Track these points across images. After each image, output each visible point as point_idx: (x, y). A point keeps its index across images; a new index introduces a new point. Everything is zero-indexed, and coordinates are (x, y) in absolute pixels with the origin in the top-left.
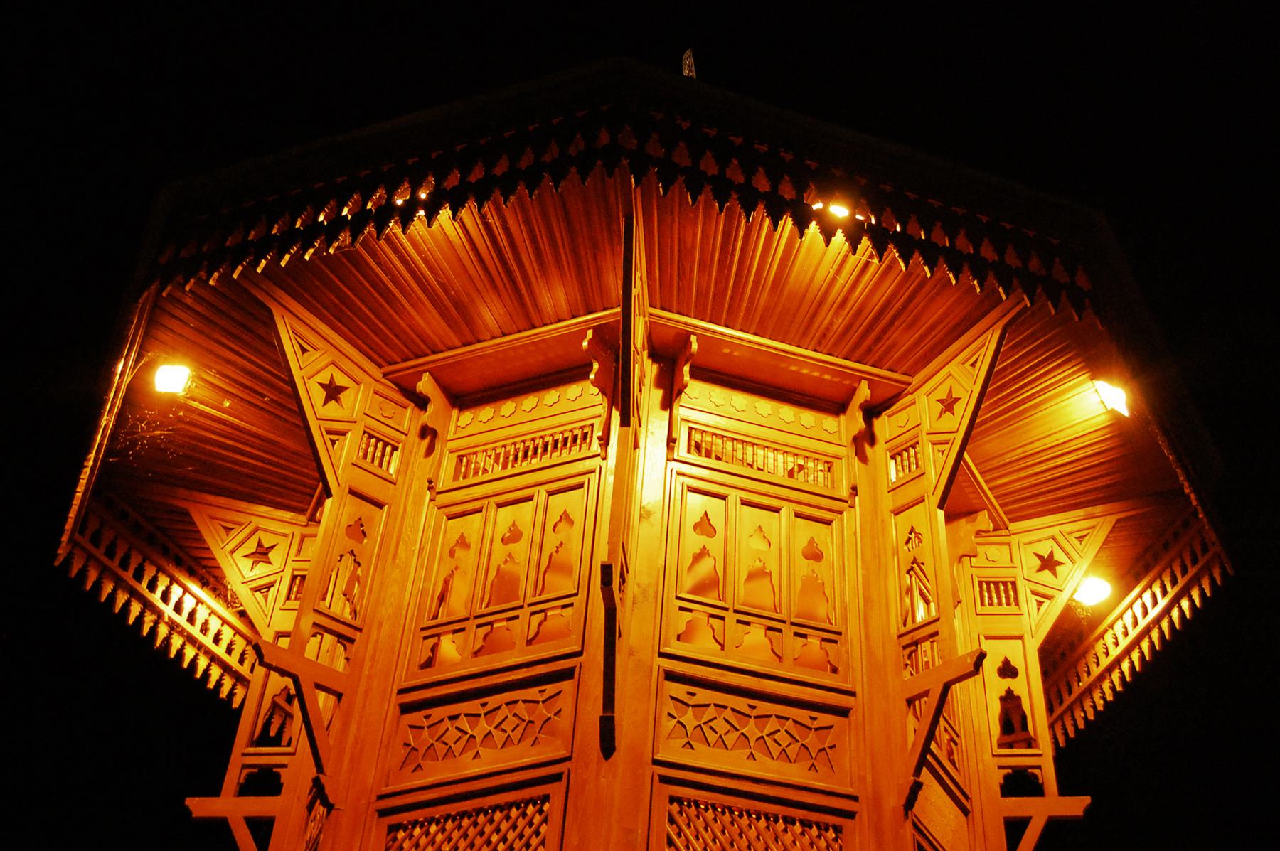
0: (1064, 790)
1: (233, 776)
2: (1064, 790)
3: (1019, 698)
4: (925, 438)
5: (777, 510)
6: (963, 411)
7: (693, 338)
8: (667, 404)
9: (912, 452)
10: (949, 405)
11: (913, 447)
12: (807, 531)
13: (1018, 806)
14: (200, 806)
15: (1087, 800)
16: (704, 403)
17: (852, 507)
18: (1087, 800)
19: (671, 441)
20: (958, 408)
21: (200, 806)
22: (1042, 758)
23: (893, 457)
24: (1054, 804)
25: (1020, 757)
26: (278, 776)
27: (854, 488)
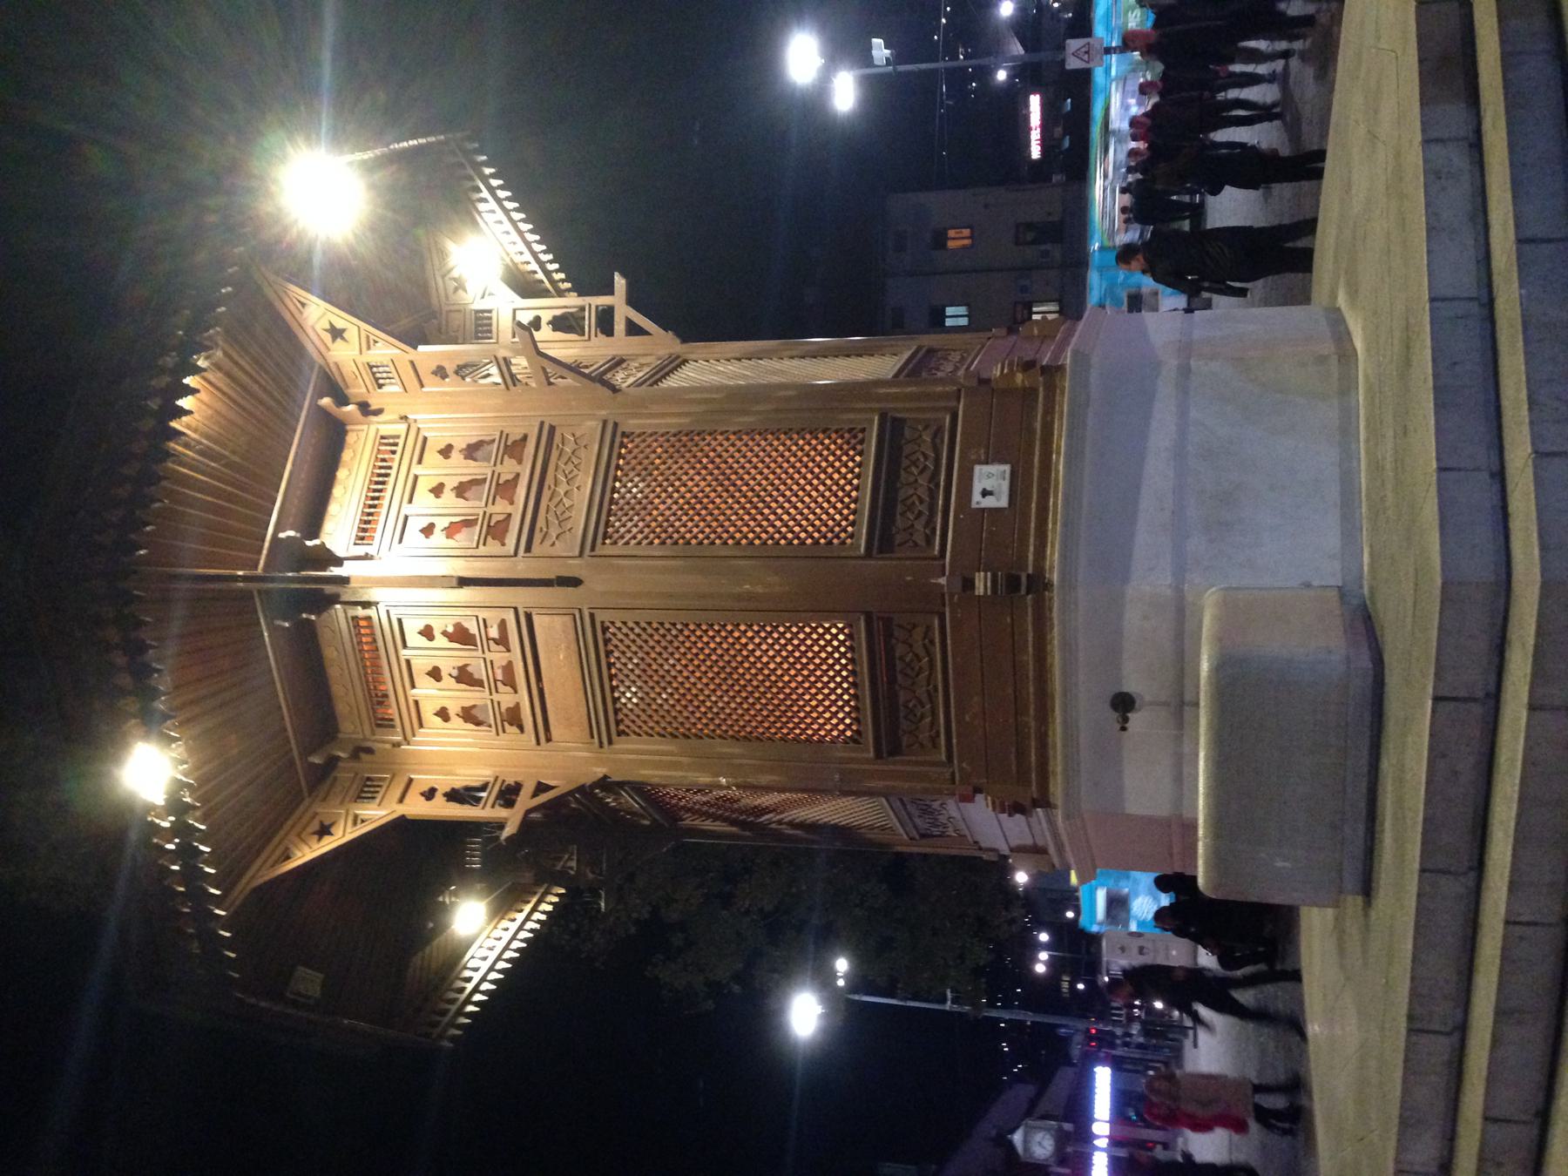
0: (611, 292)
2: (611, 292)
3: (555, 317)
5: (416, 477)
6: (341, 320)
7: (282, 535)
8: (339, 562)
10: (336, 333)
12: (432, 456)
13: (620, 326)
19: (367, 557)
20: (339, 324)
23: (380, 386)
24: (617, 299)
25: (590, 320)
27: (404, 418)
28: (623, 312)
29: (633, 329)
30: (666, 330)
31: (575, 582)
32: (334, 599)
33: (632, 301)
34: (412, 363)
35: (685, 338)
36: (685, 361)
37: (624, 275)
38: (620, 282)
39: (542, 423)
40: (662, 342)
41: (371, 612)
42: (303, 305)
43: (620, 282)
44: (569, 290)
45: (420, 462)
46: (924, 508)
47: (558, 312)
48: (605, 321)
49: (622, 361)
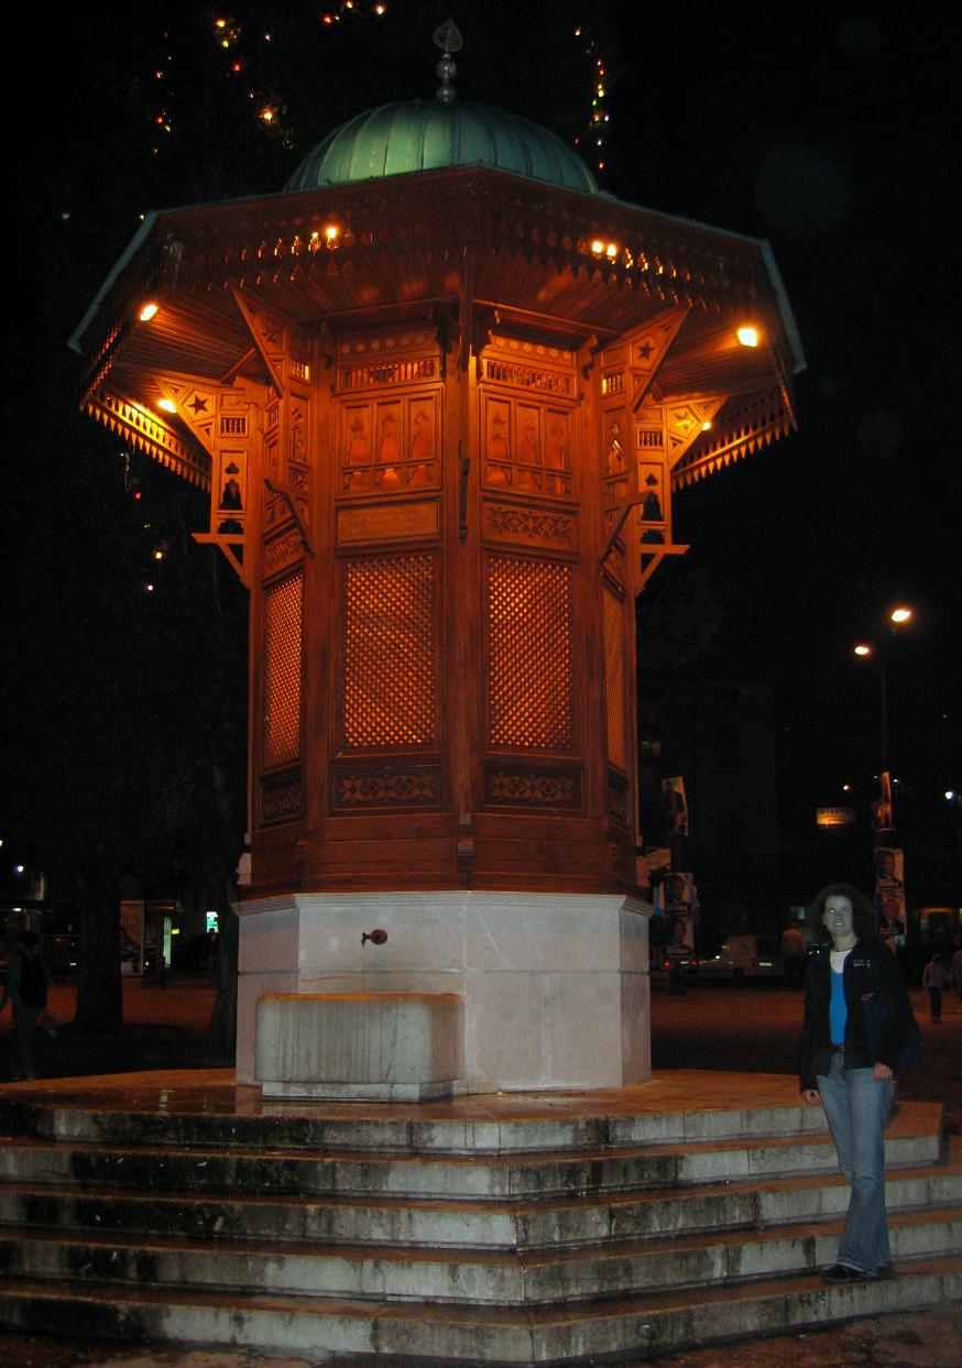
0: (676, 541)
1: (215, 523)
4: (626, 369)
9: (619, 377)
10: (646, 351)
11: (620, 374)
14: (201, 538)
15: (687, 547)
16: (499, 349)
17: (580, 405)
18: (687, 547)
21: (201, 538)
22: (664, 525)
25: (655, 525)
26: (239, 525)
27: (581, 396)
28: (660, 551)
29: (647, 559)
30: (646, 584)
31: (463, 538)
32: (446, 349)
33: (668, 559)
34: (624, 407)
35: (642, 601)
36: (622, 602)
37: (688, 551)
38: (681, 549)
39: (578, 505)
40: (638, 580)
41: (437, 376)
42: (666, 330)
43: (681, 549)
44: (678, 486)
45: (549, 410)
46: (517, 795)
47: (660, 499)
48: (654, 537)
49: (622, 552)
